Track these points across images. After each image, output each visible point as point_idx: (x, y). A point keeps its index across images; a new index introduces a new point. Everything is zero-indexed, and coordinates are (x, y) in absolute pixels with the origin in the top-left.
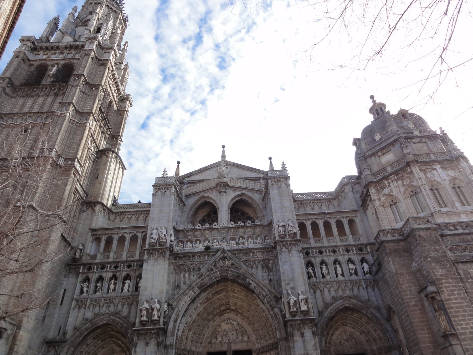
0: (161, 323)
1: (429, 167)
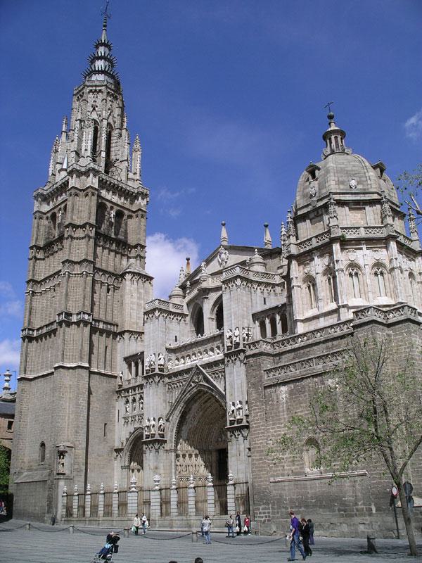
0: (157, 434)
1: (309, 258)
